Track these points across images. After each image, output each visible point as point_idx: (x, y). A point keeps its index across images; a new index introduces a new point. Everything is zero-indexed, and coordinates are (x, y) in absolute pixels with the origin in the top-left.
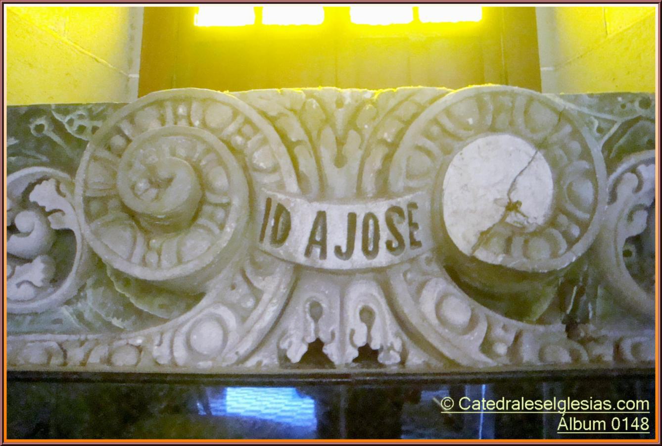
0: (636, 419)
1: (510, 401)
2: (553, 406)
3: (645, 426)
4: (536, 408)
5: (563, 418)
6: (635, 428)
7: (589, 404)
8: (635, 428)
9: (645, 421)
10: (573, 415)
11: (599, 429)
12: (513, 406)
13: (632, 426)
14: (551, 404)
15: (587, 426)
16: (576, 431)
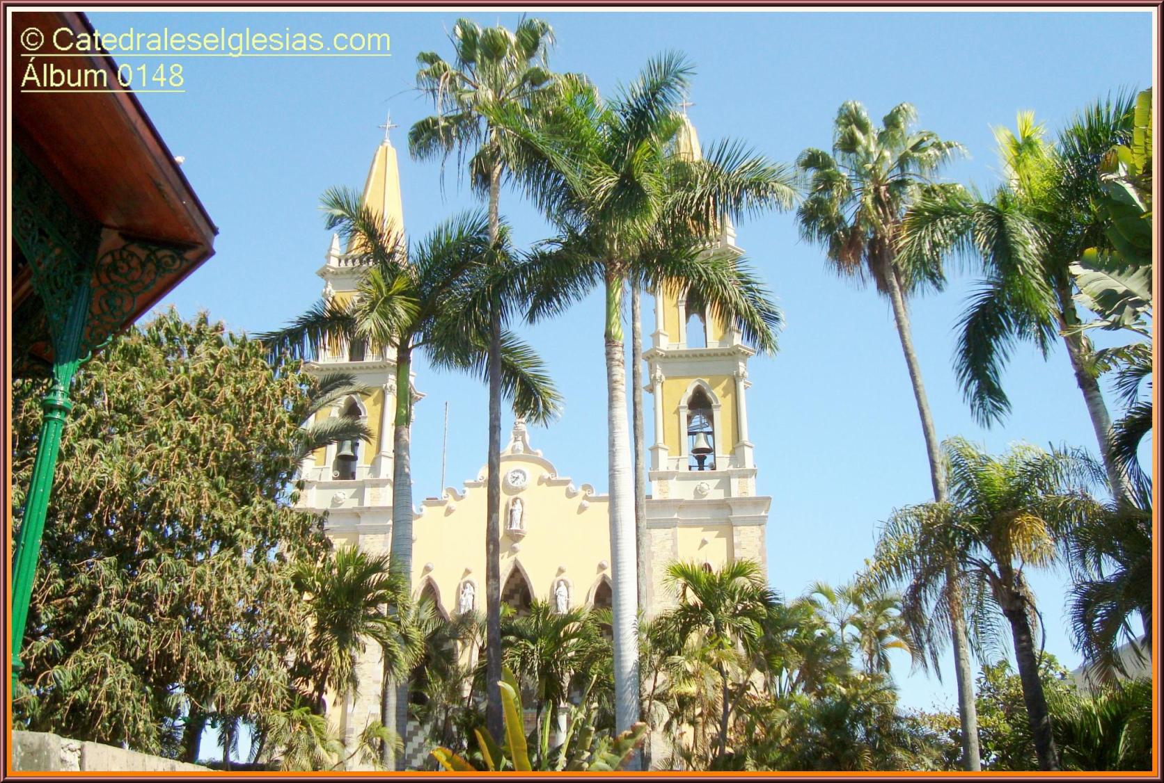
0: (162, 67)
1: (144, 35)
2: (220, 43)
3: (176, 80)
4: (272, 48)
5: (30, 65)
6: (159, 82)
7: (283, 40)
8: (159, 82)
9: (176, 70)
10: (49, 61)
11: (96, 85)
12: (149, 43)
13: (154, 79)
14: (217, 41)
15: (74, 80)
16: (54, 88)
